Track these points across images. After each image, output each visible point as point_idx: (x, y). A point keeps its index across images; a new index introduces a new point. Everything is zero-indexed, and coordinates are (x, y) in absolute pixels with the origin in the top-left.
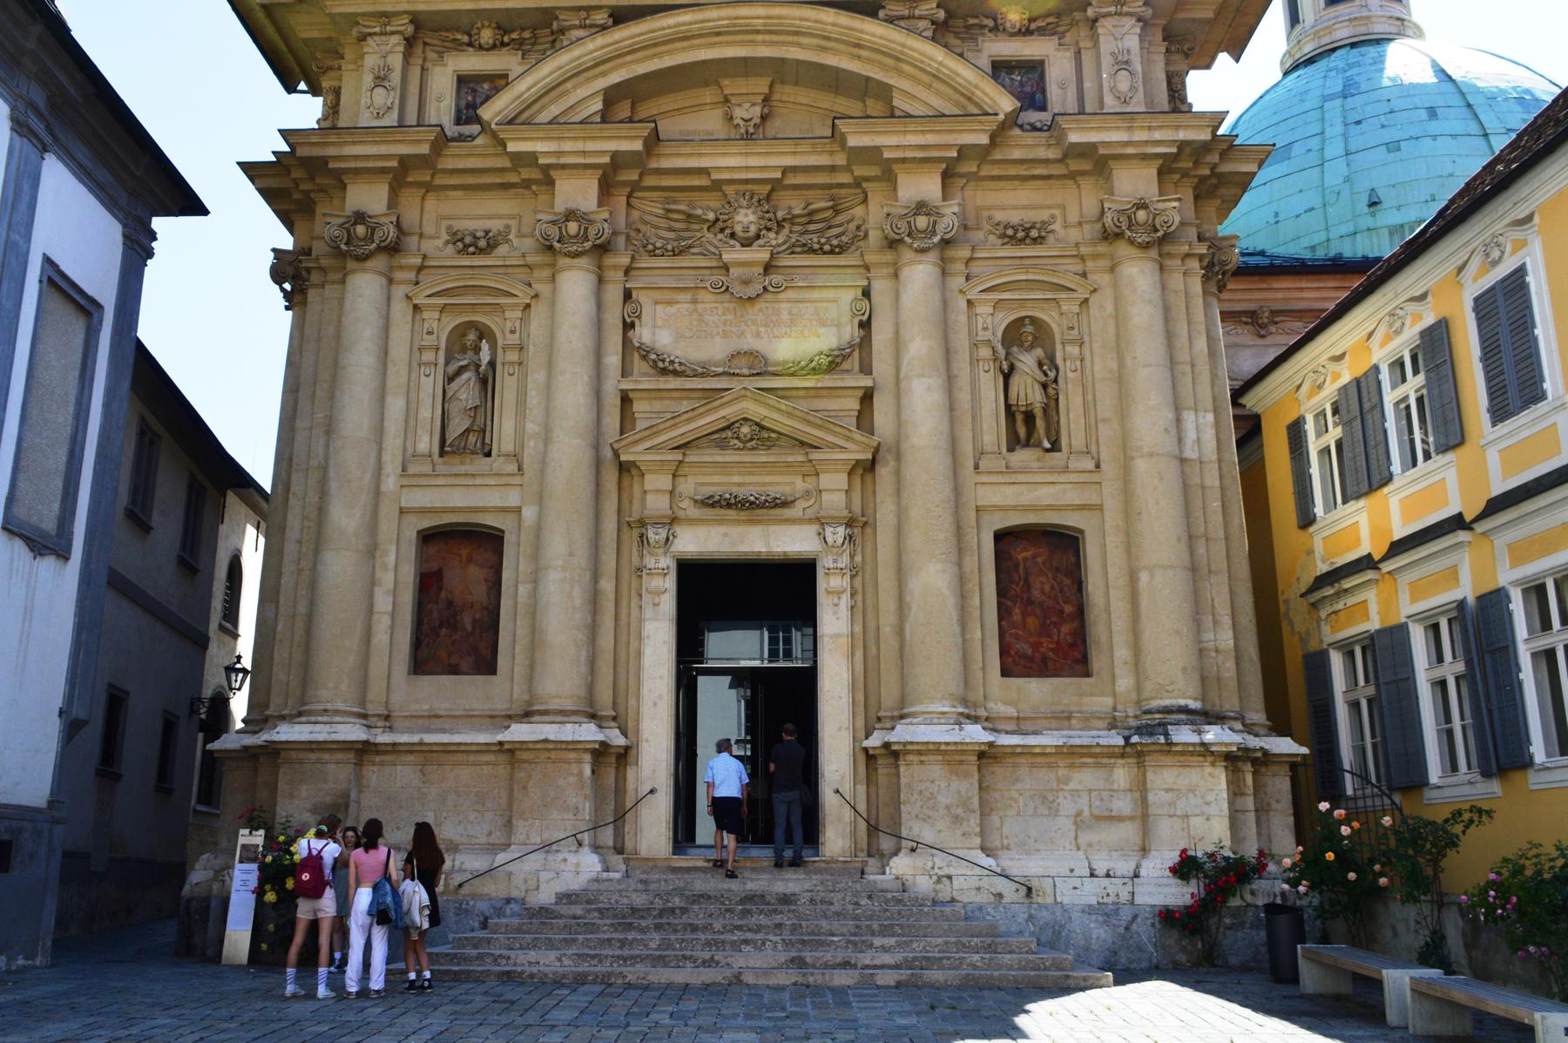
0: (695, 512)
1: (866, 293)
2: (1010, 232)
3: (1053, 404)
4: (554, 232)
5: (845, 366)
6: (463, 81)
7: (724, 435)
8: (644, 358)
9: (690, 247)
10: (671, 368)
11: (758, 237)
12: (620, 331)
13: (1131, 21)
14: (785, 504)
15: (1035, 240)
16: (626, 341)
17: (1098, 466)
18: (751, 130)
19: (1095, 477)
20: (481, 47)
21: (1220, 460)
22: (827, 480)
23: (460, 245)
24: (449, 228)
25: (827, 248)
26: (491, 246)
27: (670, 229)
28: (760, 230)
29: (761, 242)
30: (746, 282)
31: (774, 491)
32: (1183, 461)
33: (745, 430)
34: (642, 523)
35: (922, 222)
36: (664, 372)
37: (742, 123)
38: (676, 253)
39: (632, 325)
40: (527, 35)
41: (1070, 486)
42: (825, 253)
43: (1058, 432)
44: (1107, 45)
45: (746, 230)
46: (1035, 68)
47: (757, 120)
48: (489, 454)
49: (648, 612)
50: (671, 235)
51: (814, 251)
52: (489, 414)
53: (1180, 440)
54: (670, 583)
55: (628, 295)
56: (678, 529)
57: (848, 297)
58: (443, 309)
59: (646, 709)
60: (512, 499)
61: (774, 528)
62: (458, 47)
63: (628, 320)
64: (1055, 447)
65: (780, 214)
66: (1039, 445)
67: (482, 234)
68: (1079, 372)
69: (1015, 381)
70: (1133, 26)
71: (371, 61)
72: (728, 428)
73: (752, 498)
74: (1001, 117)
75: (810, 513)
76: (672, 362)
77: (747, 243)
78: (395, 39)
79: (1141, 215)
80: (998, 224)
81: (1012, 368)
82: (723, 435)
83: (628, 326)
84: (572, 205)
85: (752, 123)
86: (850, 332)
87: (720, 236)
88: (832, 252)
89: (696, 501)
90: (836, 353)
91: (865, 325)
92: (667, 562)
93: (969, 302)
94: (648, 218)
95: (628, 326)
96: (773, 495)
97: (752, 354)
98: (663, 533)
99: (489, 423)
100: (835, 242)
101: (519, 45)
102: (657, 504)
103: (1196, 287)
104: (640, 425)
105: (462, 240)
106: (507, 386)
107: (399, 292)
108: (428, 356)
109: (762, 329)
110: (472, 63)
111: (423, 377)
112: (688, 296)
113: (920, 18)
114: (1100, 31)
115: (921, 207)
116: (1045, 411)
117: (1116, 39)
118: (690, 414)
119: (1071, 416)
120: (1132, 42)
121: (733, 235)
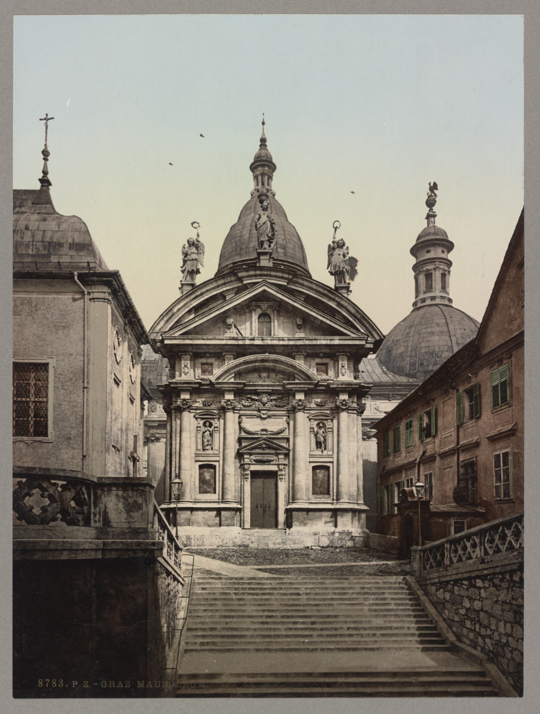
0: (254, 462)
8: (244, 430)
13: (345, 357)
14: (273, 461)
16: (240, 426)
20: (206, 357)
22: (280, 457)
30: (264, 414)
31: (270, 458)
33: (264, 446)
34: (244, 464)
35: (300, 403)
49: (245, 482)
54: (249, 477)
55: (240, 417)
56: (251, 466)
57: (285, 418)
59: (246, 500)
60: (217, 459)
61: (269, 466)
64: (325, 449)
65: (272, 398)
69: (318, 435)
75: (277, 463)
77: (264, 405)
78: (188, 356)
83: (240, 423)
84: (228, 398)
86: (286, 425)
89: (254, 461)
91: (288, 424)
92: (249, 472)
97: (266, 430)
98: (248, 466)
101: (213, 357)
102: (247, 461)
108: (199, 429)
115: (300, 400)
120: (346, 363)
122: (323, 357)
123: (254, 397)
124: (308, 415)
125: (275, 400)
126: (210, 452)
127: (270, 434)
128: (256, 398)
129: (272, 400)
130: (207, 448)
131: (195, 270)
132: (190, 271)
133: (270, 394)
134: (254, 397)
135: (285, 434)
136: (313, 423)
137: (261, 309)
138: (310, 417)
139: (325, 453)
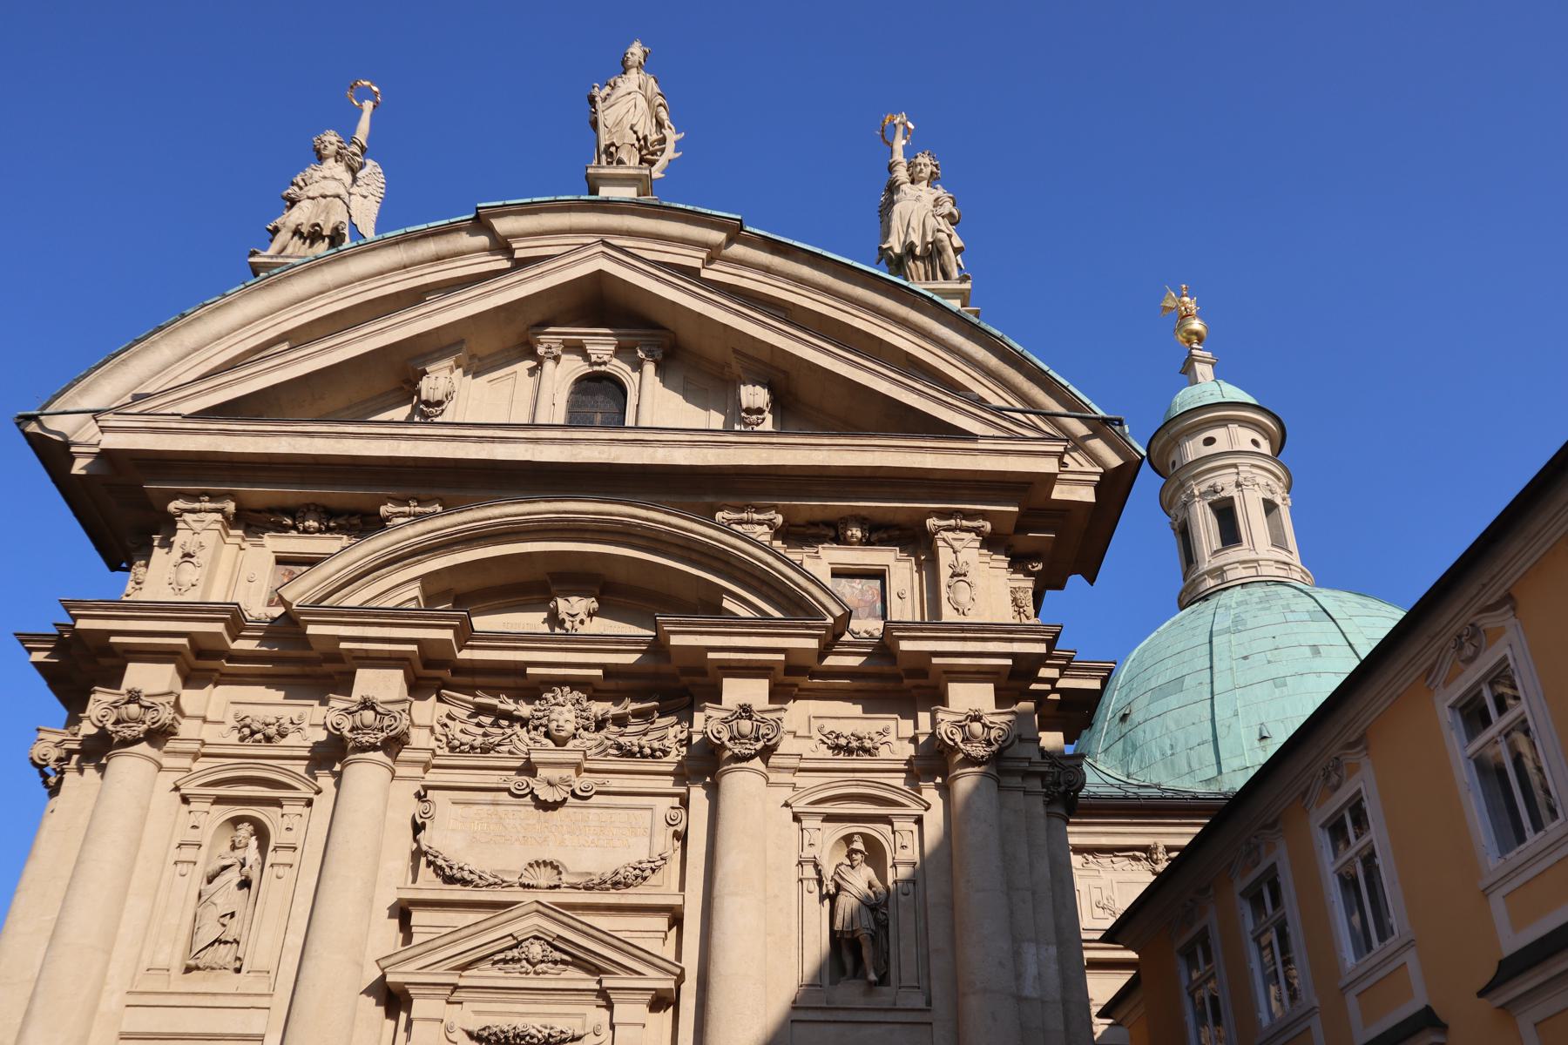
1: (685, 802)
2: (843, 742)
3: (882, 933)
4: (346, 725)
5: (653, 880)
6: (281, 561)
7: (510, 954)
9: (499, 745)
10: (458, 875)
11: (574, 736)
12: (411, 832)
15: (867, 751)
17: (929, 1003)
18: (577, 624)
19: (925, 1018)
20: (306, 531)
21: (1065, 1002)
23: (247, 731)
24: (236, 716)
25: (647, 751)
26: (283, 736)
27: (479, 725)
28: (577, 729)
29: (578, 742)
32: (1020, 999)
33: (536, 950)
35: (746, 726)
36: (450, 880)
37: (567, 618)
38: (485, 750)
39: (424, 825)
40: (355, 521)
41: (898, 1026)
42: (644, 756)
43: (887, 963)
44: (945, 557)
45: (559, 729)
46: (879, 575)
47: (583, 616)
48: (238, 971)
50: (481, 731)
51: (633, 755)
52: (247, 922)
53: (1018, 976)
58: (219, 800)
62: (283, 529)
63: (419, 821)
64: (883, 980)
66: (865, 976)
67: (274, 721)
68: (911, 896)
70: (974, 540)
71: (182, 538)
72: (516, 946)
73: (534, 1032)
74: (830, 620)
76: (461, 869)
77: (560, 742)
79: (976, 727)
80: (831, 733)
81: (838, 887)
82: (509, 954)
83: (418, 828)
84: (370, 693)
85: (578, 619)
86: (664, 841)
87: (533, 733)
88: (653, 756)
89: (470, 1035)
90: (644, 865)
91: (682, 837)
93: (796, 818)
94: (456, 711)
95: (418, 828)
96: (559, 1028)
99: (245, 933)
100: (656, 745)
103: (1038, 805)
104: (416, 940)
105: (249, 726)
106: (272, 888)
107: (168, 780)
108: (188, 853)
109: (566, 836)
110: (293, 544)
111: (178, 878)
112: (489, 796)
113: (760, 523)
114: (940, 543)
115: (746, 711)
116: (874, 938)
117: (955, 552)
118: (472, 930)
119: (901, 944)
121: (547, 735)
122: (867, 542)
123: (509, 705)
124: (787, 793)
125: (620, 721)
126: (229, 982)
127: (573, 887)
128: (525, 710)
129: (600, 725)
130: (207, 958)
131: (327, 232)
132: (305, 229)
133: (592, 689)
134: (509, 705)
135: (662, 890)
136: (817, 837)
137: (586, 357)
138: (800, 806)
139: (886, 995)
